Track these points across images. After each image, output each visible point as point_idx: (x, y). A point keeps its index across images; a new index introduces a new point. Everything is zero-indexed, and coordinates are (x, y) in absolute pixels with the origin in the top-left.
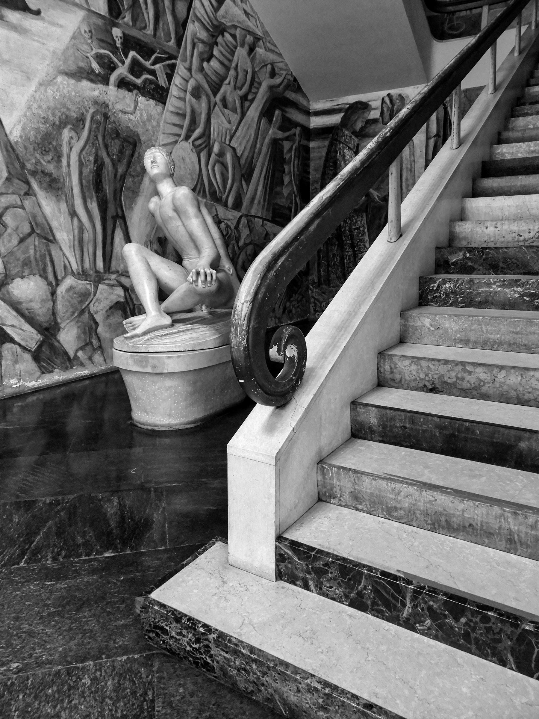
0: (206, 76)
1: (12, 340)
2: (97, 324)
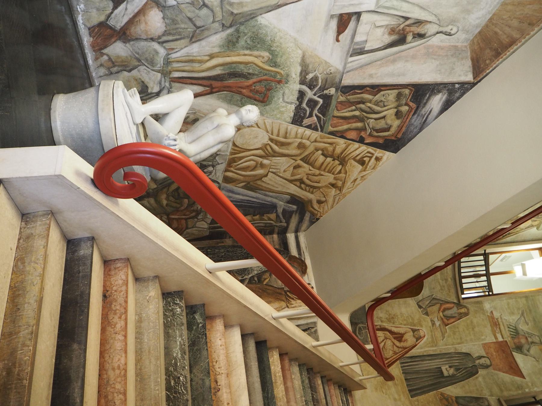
0: (313, 153)
1: (115, 7)
2: (130, 71)
